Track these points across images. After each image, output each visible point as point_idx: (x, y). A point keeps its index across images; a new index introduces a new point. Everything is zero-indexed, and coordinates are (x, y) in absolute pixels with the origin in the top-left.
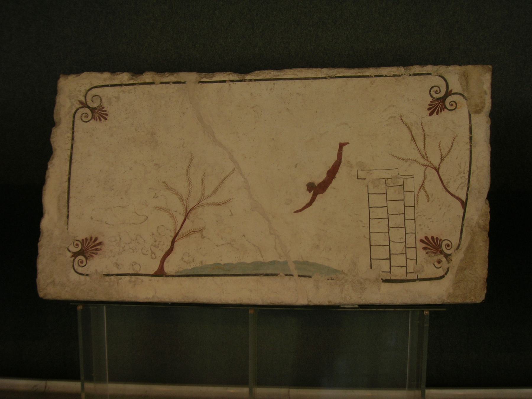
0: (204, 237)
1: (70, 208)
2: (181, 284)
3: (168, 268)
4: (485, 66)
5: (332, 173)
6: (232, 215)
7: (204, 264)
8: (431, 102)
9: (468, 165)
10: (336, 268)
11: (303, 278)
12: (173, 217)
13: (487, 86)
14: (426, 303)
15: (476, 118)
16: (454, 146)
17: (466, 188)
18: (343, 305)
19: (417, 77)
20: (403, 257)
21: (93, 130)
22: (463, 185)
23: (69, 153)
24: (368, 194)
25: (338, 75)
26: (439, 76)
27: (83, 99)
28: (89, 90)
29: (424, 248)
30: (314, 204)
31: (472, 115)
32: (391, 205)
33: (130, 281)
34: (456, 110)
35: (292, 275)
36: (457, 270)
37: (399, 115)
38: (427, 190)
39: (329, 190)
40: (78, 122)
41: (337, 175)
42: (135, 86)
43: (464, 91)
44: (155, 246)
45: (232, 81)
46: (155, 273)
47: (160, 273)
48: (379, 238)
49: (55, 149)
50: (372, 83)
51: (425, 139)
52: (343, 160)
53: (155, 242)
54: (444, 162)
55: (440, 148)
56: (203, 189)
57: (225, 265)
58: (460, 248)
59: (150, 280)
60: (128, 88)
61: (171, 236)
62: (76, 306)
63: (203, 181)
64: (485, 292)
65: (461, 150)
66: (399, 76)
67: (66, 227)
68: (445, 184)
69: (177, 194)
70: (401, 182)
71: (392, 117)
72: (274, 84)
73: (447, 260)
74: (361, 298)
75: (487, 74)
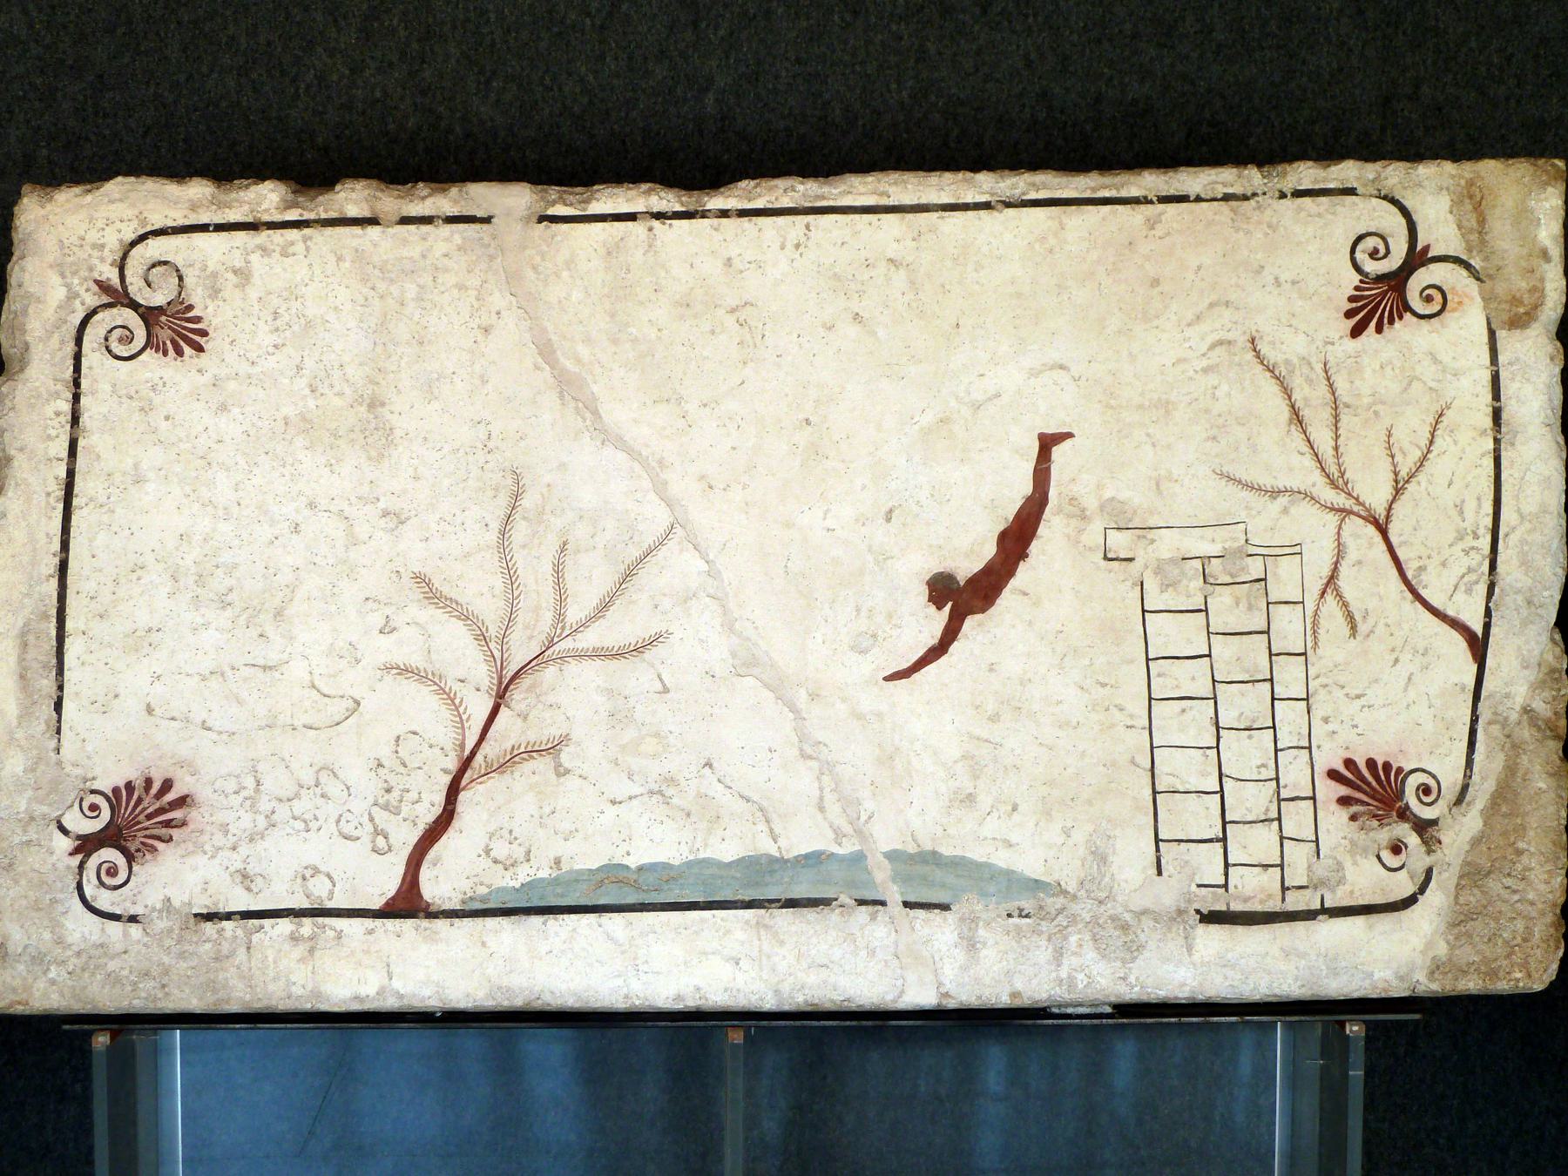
0: (567, 771)
1: (67, 673)
2: (484, 944)
3: (437, 886)
4: (1541, 162)
5: (1017, 538)
6: (666, 690)
7: (565, 867)
8: (1357, 288)
9: (1488, 508)
10: (1034, 876)
13: (1548, 233)
14: (1356, 995)
15: (1514, 346)
16: (1438, 441)
17: (1482, 589)
18: (1060, 1006)
19: (1307, 200)
20: (1269, 834)
22: (1473, 577)
23: (64, 475)
24: (1144, 611)
25: (1033, 196)
26: (1385, 198)
27: (112, 275)
28: (133, 244)
29: (1344, 801)
30: (955, 647)
31: (1501, 334)
33: (294, 938)
34: (1446, 315)
35: (883, 903)
36: (1461, 877)
37: (1248, 337)
39: (1008, 598)
40: (93, 358)
41: (1034, 548)
42: (307, 231)
43: (1470, 250)
44: (386, 807)
45: (659, 216)
46: (387, 904)
47: (407, 904)
50: (1151, 224)
51: (1336, 417)
52: (1052, 494)
53: (388, 791)
54: (1405, 497)
56: (561, 598)
57: (640, 869)
58: (1468, 798)
59: (370, 932)
60: (278, 236)
61: (445, 771)
62: (89, 1034)
63: (558, 570)
64: (1561, 953)
65: (1462, 458)
66: (1245, 198)
67: (53, 744)
69: (465, 617)
70: (1255, 568)
71: (1220, 343)
73: (1425, 842)
74: (1124, 979)
75: (1550, 189)
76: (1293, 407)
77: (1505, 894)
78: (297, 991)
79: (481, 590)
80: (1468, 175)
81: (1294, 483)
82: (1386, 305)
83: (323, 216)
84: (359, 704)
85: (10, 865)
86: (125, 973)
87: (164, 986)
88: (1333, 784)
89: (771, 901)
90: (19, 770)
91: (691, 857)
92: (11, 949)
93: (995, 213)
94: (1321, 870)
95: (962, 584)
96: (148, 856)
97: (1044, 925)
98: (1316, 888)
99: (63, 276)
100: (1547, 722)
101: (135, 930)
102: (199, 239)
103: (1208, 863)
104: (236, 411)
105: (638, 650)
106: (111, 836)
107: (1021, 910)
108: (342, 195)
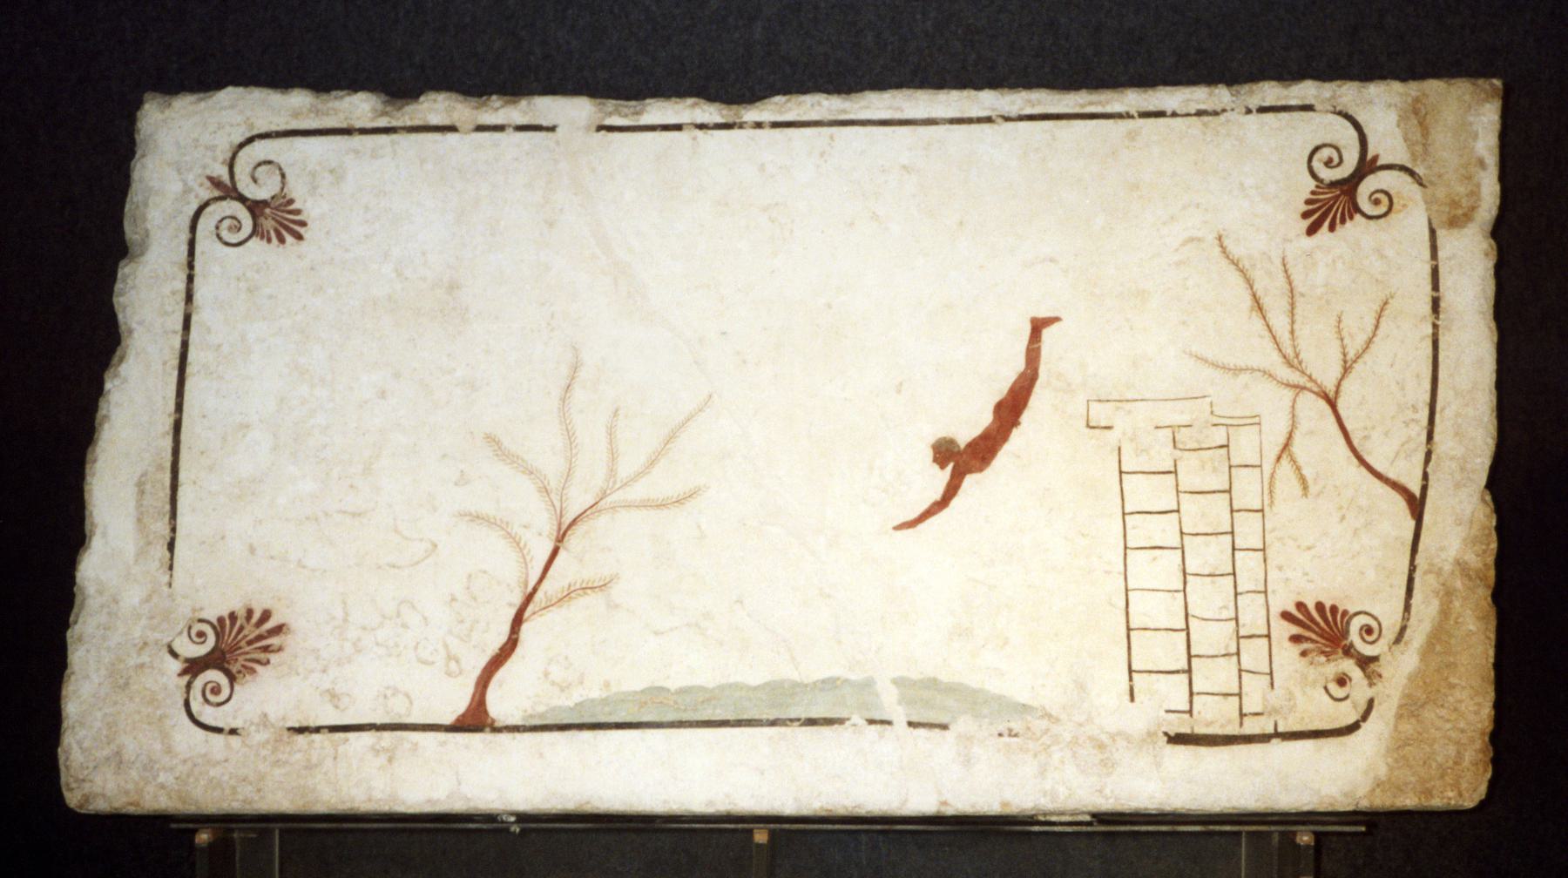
0: (617, 606)
2: (541, 755)
3: (500, 706)
4: (1481, 82)
5: (1011, 409)
7: (614, 689)
8: (1313, 193)
9: (1427, 386)
10: (1022, 700)
11: (921, 732)
12: (516, 542)
14: (1306, 808)
17: (1421, 456)
19: (1269, 117)
21: (258, 271)
23: (177, 342)
25: (1028, 111)
26: (1340, 113)
27: (223, 173)
28: (241, 146)
29: (1296, 639)
30: (955, 502)
31: (1441, 233)
32: (1189, 505)
34: (1392, 216)
35: (889, 723)
36: (1401, 706)
38: (1301, 461)
40: (206, 244)
41: (1025, 417)
42: (394, 137)
43: (1414, 160)
45: (702, 127)
46: (458, 720)
47: (474, 720)
48: (1156, 609)
49: (130, 332)
51: (1293, 305)
55: (1339, 331)
56: (613, 455)
58: (1406, 637)
61: (510, 605)
62: (194, 832)
63: (611, 432)
64: (1489, 775)
66: (1216, 113)
67: (166, 578)
68: (1356, 442)
70: (1219, 436)
71: (1192, 240)
72: (832, 138)
73: (1368, 677)
74: (1100, 791)
75: (1488, 106)
76: (1254, 295)
77: (1439, 723)
78: (377, 795)
79: (543, 447)
80: (1414, 93)
81: (1254, 361)
82: (1339, 208)
83: (409, 123)
84: (435, 546)
85: (127, 684)
86: (226, 778)
87: (259, 791)
88: (1285, 623)
89: (791, 720)
90: (136, 600)
91: (723, 681)
92: (126, 757)
93: (995, 127)
94: (1277, 698)
95: (962, 446)
96: (248, 677)
97: (1031, 745)
98: (1270, 714)
99: (179, 171)
100: (1477, 572)
101: (233, 739)
102: (299, 142)
103: (1174, 692)
104: (331, 291)
105: (679, 501)
106: (217, 659)
107: (1010, 730)
108: (426, 105)
